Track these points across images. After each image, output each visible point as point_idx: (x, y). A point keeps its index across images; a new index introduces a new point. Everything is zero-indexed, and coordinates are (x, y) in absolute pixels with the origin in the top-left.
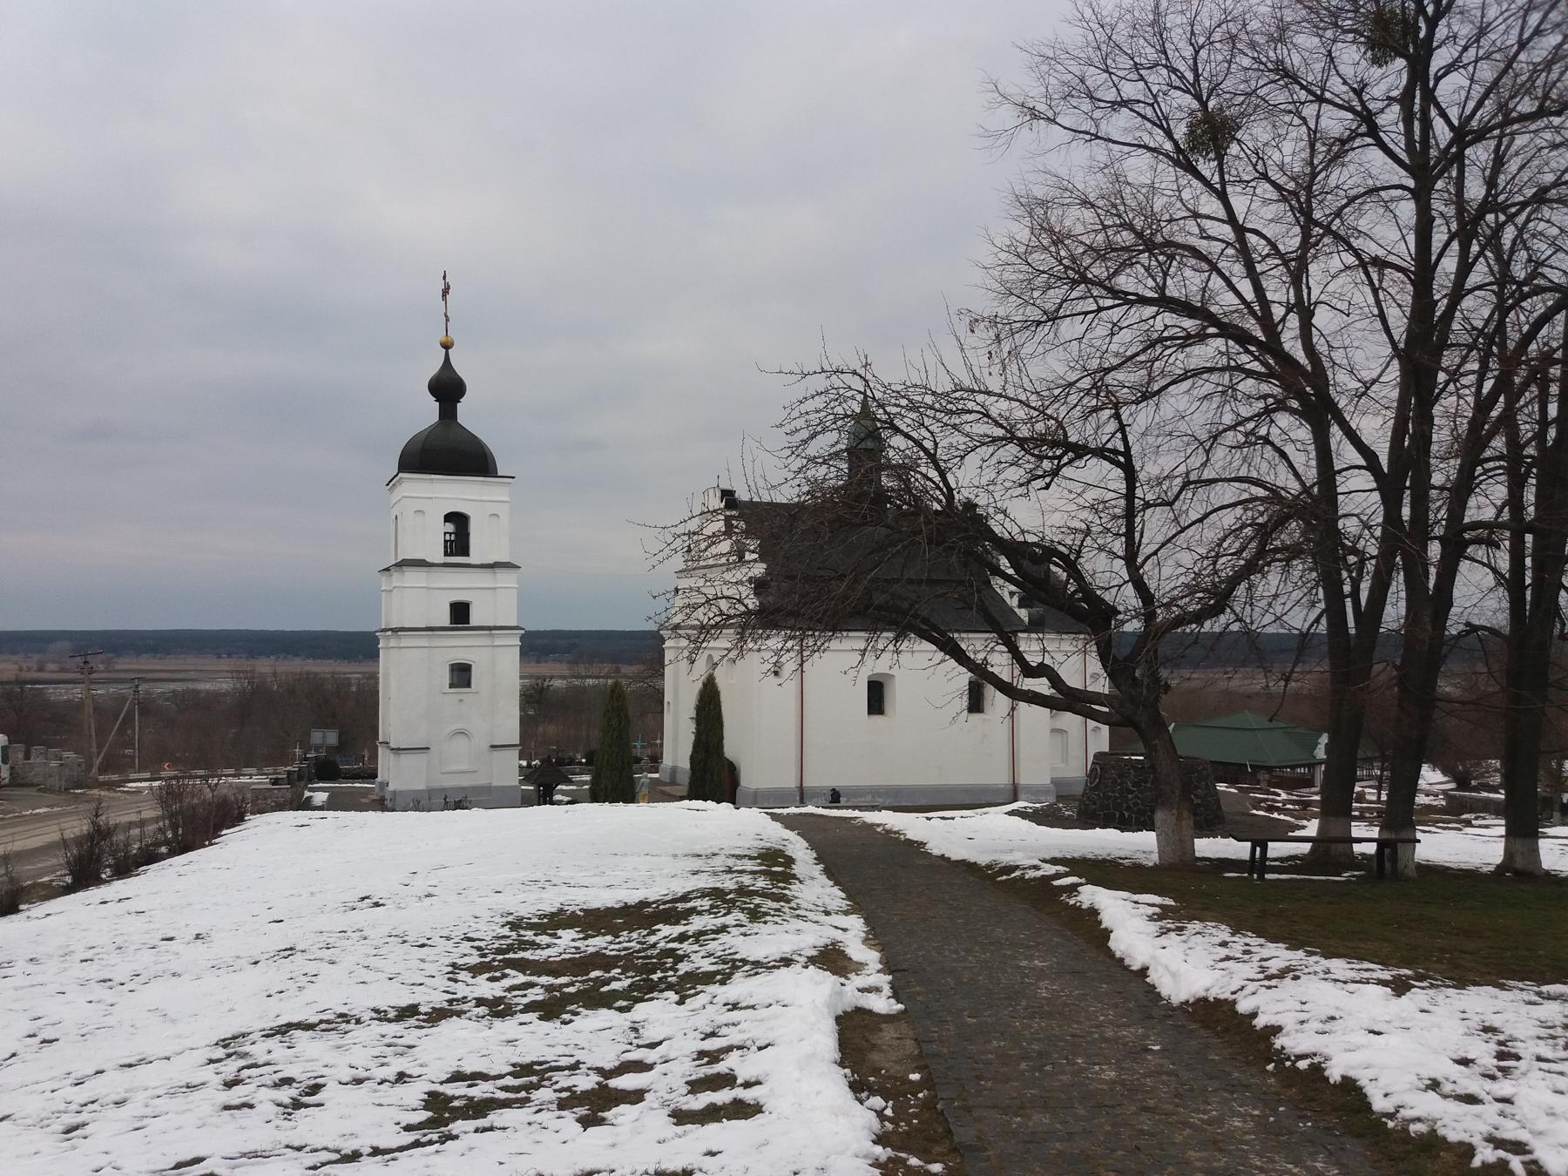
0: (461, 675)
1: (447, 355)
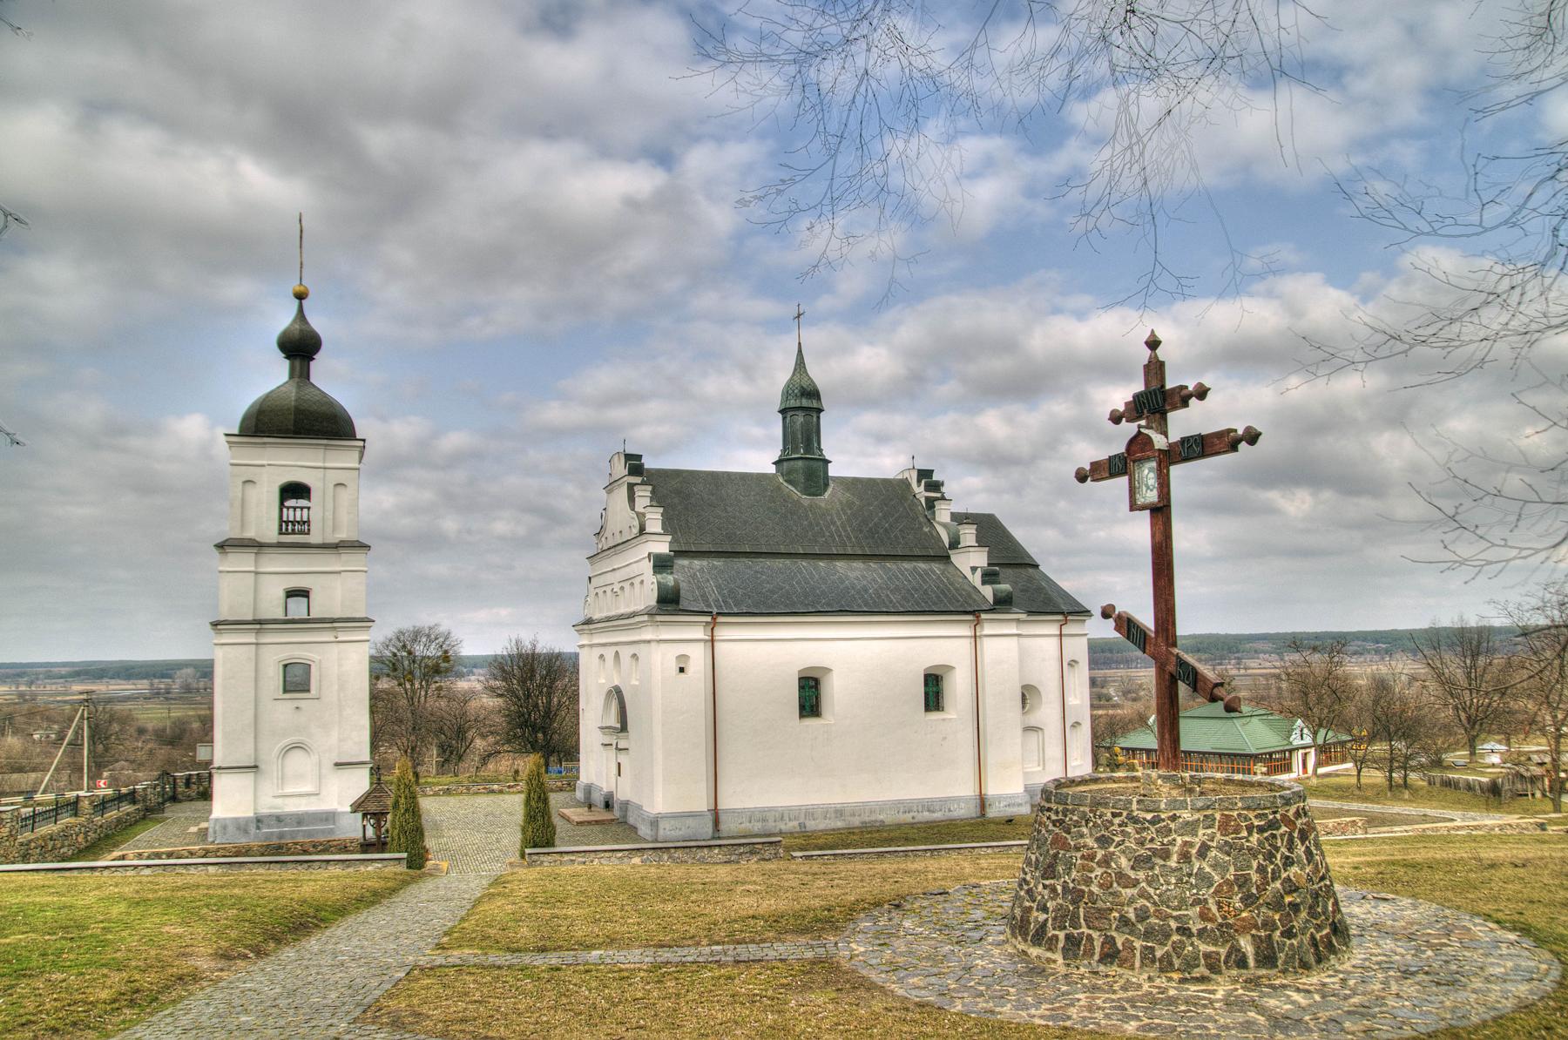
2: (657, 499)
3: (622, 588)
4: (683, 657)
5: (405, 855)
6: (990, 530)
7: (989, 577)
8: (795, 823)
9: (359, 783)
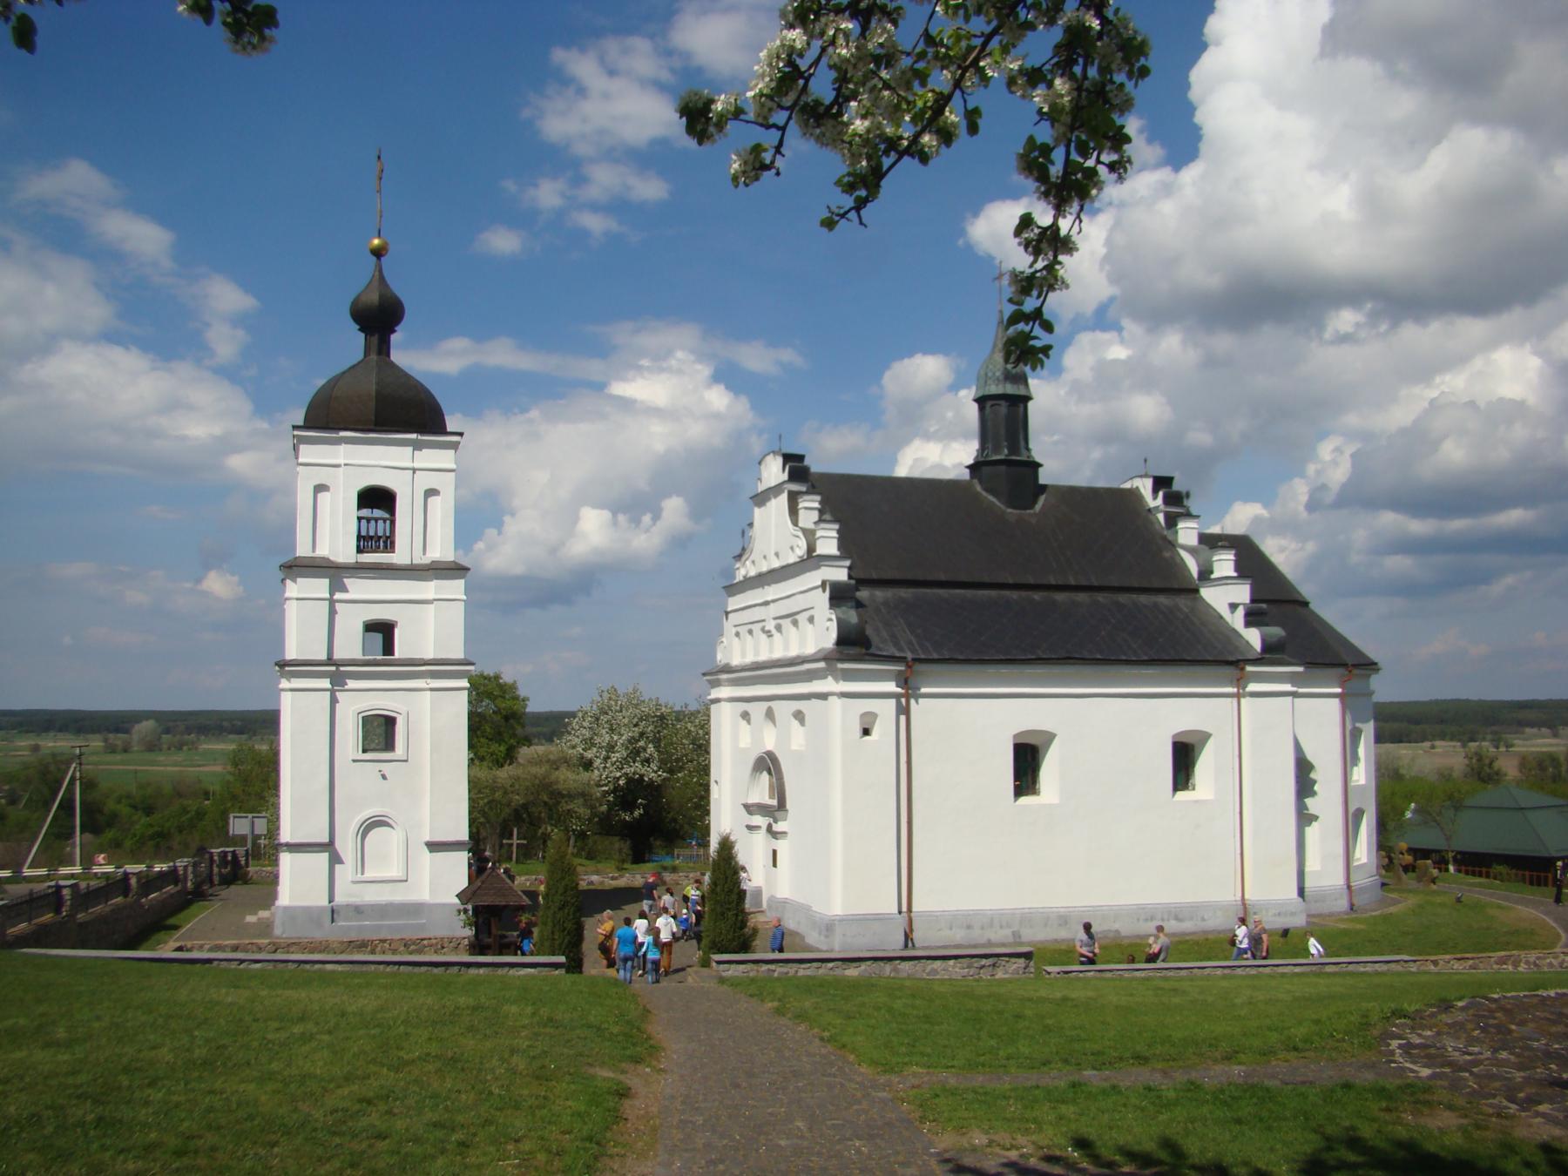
0: (380, 733)
2: (829, 511)
3: (779, 628)
5: (562, 959)
6: (1251, 562)
7: (1252, 618)
8: (1008, 932)
9: (455, 872)
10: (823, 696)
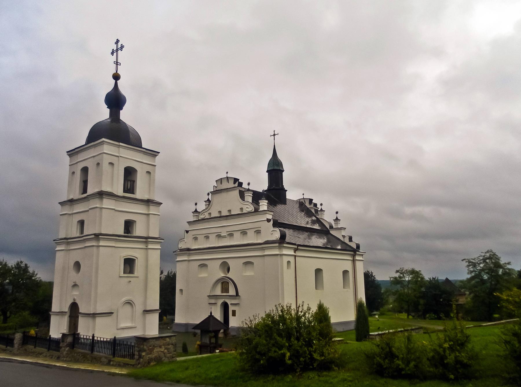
1: (116, 84)
3: (231, 235)
4: (289, 262)
10: (277, 255)
